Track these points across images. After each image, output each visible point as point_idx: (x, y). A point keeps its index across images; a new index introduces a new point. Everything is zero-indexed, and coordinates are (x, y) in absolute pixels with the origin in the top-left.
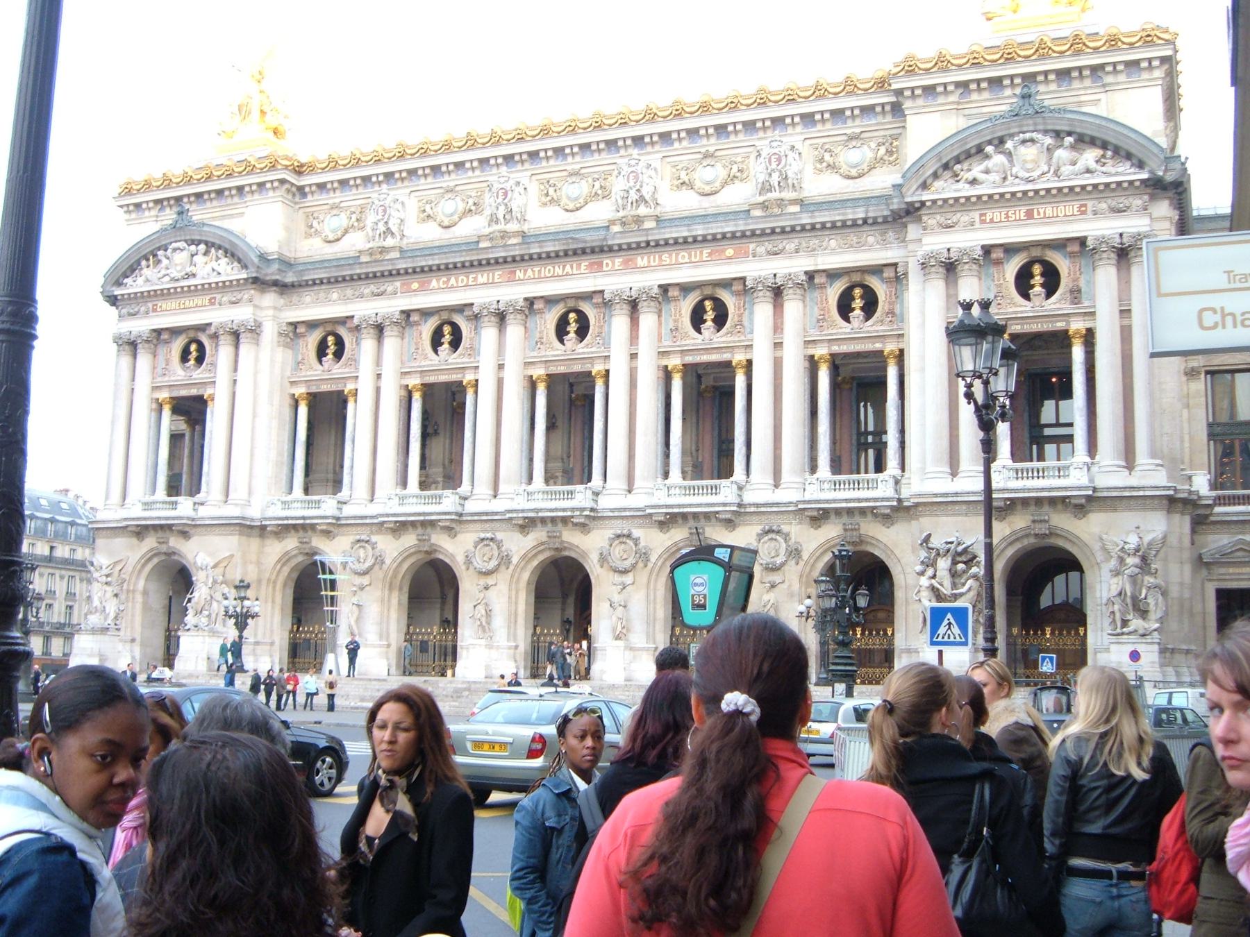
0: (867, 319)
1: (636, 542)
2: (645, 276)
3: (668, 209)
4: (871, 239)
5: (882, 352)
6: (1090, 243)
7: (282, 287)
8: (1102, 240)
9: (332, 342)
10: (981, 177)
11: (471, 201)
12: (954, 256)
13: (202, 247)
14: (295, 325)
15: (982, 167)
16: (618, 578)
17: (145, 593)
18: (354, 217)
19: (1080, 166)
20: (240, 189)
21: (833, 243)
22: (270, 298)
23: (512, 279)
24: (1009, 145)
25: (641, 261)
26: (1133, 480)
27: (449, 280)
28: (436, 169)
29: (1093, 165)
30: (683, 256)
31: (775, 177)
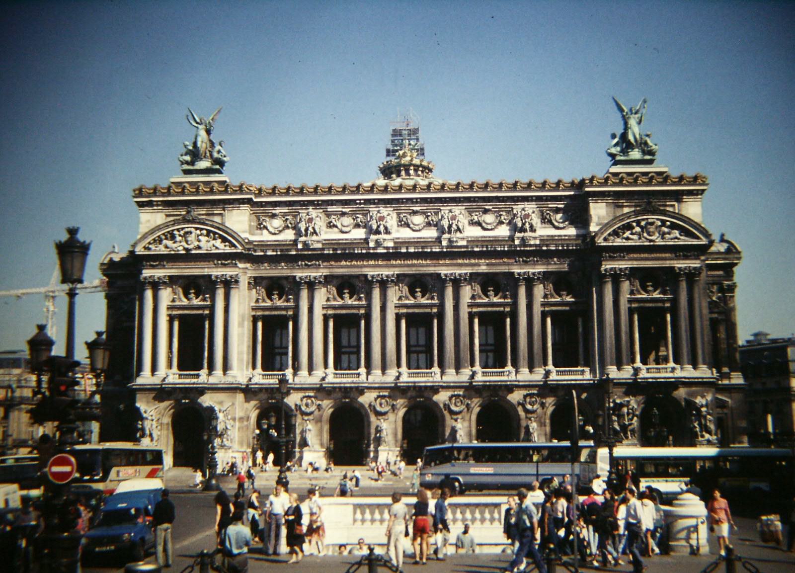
10: (631, 236)
11: (359, 220)
14: (255, 278)
19: (672, 236)
24: (643, 223)
29: (679, 236)
31: (527, 226)
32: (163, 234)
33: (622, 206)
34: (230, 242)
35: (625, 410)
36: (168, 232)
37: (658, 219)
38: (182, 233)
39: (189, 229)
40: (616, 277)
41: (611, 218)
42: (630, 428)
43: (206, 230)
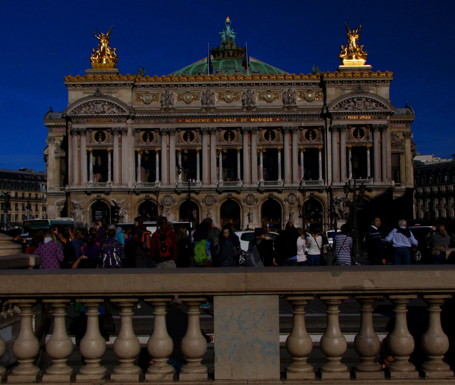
0: (313, 140)
1: (254, 196)
2: (254, 123)
3: (258, 105)
4: (316, 119)
5: (317, 149)
6: (373, 126)
7: (133, 118)
8: (376, 125)
9: (148, 134)
10: (348, 107)
11: (196, 96)
12: (341, 126)
13: (107, 103)
14: (136, 129)
15: (348, 105)
16: (249, 206)
17: (90, 212)
18: (155, 97)
19: (371, 107)
20: (116, 85)
21: (306, 119)
22: (129, 121)
23: (212, 121)
25: (252, 120)
26: (383, 184)
27: (192, 120)
28: (184, 85)
30: (265, 120)
32: (83, 104)
33: (345, 89)
34: (122, 109)
35: (341, 204)
36: (86, 103)
37: (364, 97)
38: (94, 103)
39: (98, 102)
40: (339, 129)
41: (338, 96)
42: (344, 213)
43: (108, 102)
